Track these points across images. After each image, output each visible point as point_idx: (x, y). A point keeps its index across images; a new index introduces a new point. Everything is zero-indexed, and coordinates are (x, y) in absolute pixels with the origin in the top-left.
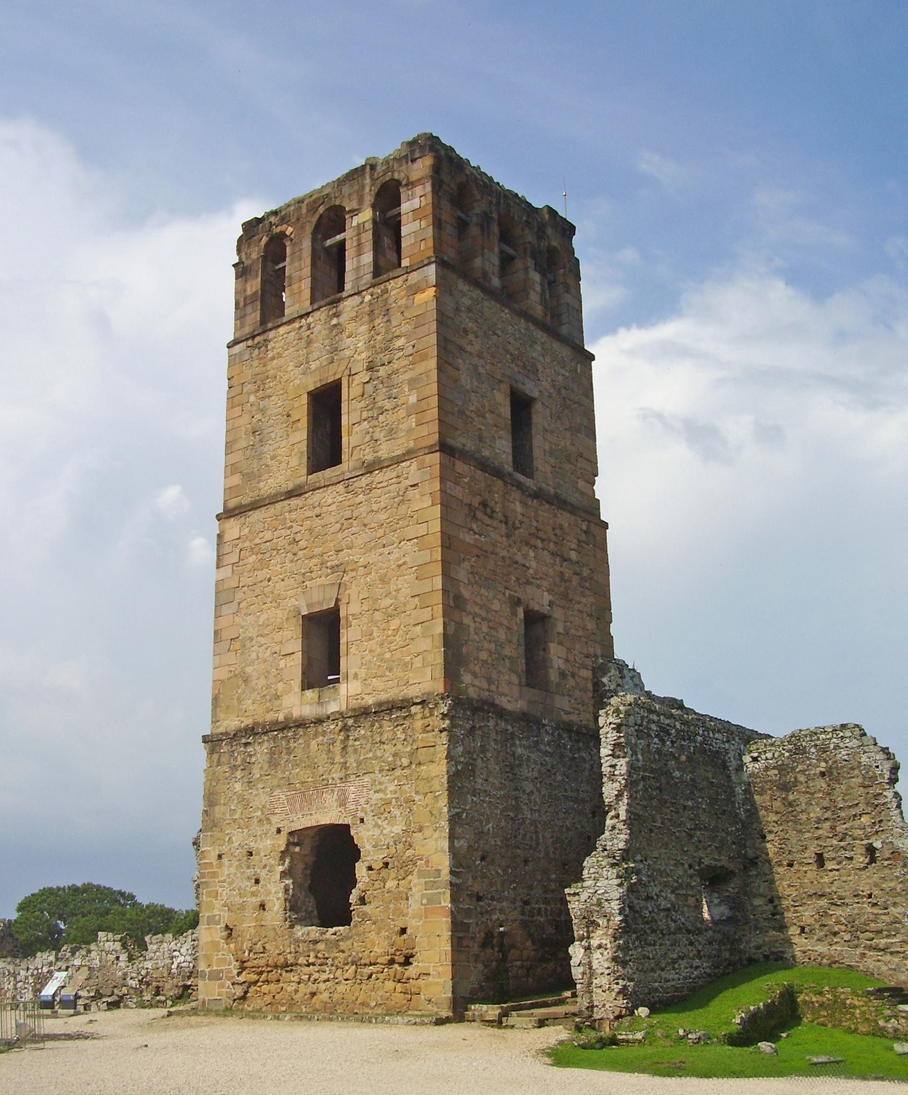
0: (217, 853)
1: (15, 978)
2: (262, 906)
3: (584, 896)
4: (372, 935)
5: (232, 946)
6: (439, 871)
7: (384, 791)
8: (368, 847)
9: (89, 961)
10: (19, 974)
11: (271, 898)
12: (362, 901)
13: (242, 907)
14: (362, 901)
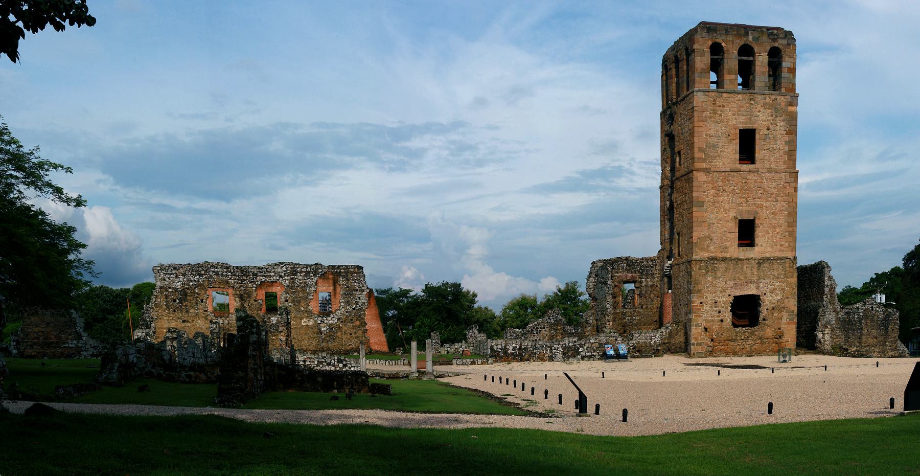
0: (700, 301)
1: (551, 349)
2: (722, 321)
3: (825, 320)
4: (768, 330)
5: (708, 334)
6: (793, 311)
7: (774, 285)
8: (767, 303)
9: (599, 341)
10: (553, 346)
11: (726, 318)
12: (764, 319)
13: (713, 321)
14: (764, 319)
